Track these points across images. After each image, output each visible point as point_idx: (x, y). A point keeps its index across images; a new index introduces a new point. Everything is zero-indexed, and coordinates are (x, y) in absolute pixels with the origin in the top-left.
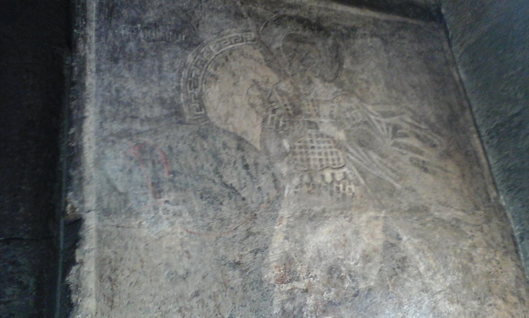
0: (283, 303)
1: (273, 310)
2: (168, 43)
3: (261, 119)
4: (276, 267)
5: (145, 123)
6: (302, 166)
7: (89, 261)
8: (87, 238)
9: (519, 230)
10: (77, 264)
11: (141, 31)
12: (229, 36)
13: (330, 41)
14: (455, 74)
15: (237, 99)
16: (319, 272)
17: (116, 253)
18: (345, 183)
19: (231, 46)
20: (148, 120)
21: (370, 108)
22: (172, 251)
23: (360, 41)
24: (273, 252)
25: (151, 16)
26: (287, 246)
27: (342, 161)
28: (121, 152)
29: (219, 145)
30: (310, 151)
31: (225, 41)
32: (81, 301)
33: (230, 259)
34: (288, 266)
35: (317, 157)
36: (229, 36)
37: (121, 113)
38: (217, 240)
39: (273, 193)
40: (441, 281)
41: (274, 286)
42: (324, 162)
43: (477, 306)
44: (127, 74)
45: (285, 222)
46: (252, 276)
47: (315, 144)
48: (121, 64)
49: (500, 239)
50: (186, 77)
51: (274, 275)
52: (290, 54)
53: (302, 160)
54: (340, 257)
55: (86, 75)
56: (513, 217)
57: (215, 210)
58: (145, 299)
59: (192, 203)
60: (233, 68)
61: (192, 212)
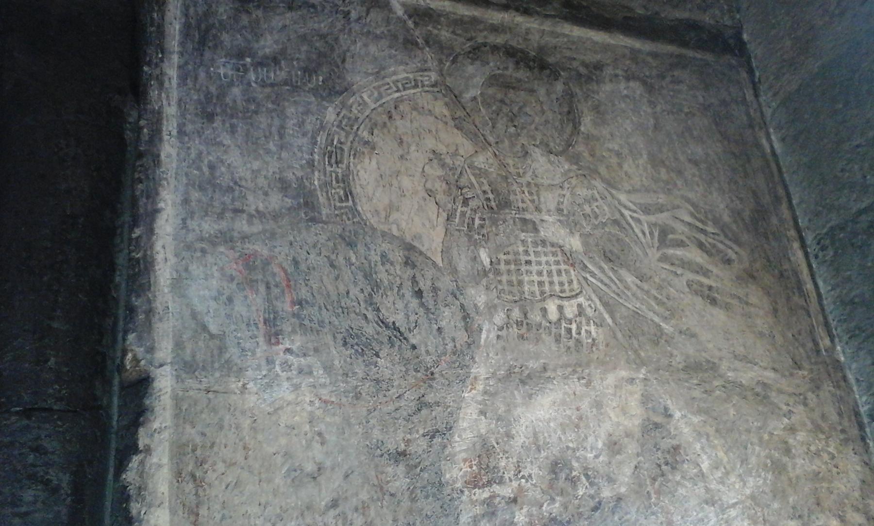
0: (475, 521)
2: (295, 88)
3: (445, 215)
4: (465, 460)
5: (256, 221)
6: (510, 292)
7: (160, 449)
9: (867, 403)
10: (141, 451)
11: (252, 69)
12: (394, 78)
13: (559, 87)
14: (764, 142)
15: (406, 182)
16: (534, 470)
17: (203, 434)
18: (581, 323)
19: (397, 95)
20: (260, 214)
21: (623, 197)
22: (295, 432)
23: (608, 87)
25: (267, 45)
26: (483, 426)
27: (575, 285)
28: (216, 268)
29: (375, 258)
30: (524, 268)
31: (387, 87)
32: (145, 513)
34: (486, 460)
35: (536, 278)
36: (394, 78)
37: (216, 204)
39: (462, 337)
40: (737, 487)
41: (462, 492)
42: (547, 288)
44: (227, 141)
45: (480, 387)
46: (426, 475)
47: (532, 258)
48: (218, 123)
49: (834, 418)
50: (323, 146)
51: (461, 473)
52: (494, 108)
53: (510, 283)
54: (571, 445)
55: (161, 140)
56: (857, 380)
57: (366, 366)
58: (249, 512)
59: (328, 353)
60: (400, 132)
61: (328, 368)
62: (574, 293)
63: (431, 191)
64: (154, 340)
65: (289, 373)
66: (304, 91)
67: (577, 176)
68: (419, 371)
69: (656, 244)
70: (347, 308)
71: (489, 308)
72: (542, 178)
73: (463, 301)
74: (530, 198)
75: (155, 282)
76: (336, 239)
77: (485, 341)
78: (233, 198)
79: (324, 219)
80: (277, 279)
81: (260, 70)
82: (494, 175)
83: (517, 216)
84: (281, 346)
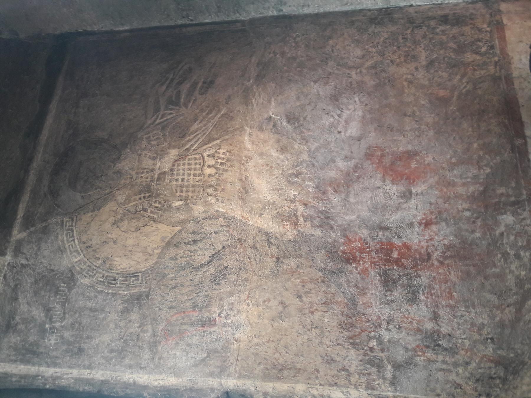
1: (318, 235)
2: (67, 300)
3: (151, 222)
4: (284, 228)
6: (199, 192)
8: (244, 388)
15: (130, 242)
17: (259, 363)
18: (218, 157)
19: (76, 241)
21: (149, 122)
24: (271, 229)
26: (267, 216)
31: (71, 246)
33: (274, 266)
35: (192, 177)
36: (66, 242)
37: (133, 350)
38: (257, 275)
39: (221, 221)
41: (299, 231)
42: (197, 172)
43: (332, 63)
45: (247, 215)
46: (289, 248)
47: (180, 178)
54: (280, 172)
57: (231, 274)
59: (223, 293)
60: (99, 242)
61: (231, 294)
62: (202, 158)
63: (136, 229)
64: (207, 388)
65: (231, 315)
66: (69, 295)
67: (134, 145)
68: (237, 246)
69: (178, 108)
70: (199, 281)
71: (206, 205)
72: (134, 165)
73: (201, 218)
74: (145, 174)
75: (176, 386)
76: (160, 284)
77: (224, 209)
78: (130, 340)
79: (148, 290)
80: (180, 318)
81: (54, 320)
82: (130, 192)
83: (155, 182)
84: (217, 319)
